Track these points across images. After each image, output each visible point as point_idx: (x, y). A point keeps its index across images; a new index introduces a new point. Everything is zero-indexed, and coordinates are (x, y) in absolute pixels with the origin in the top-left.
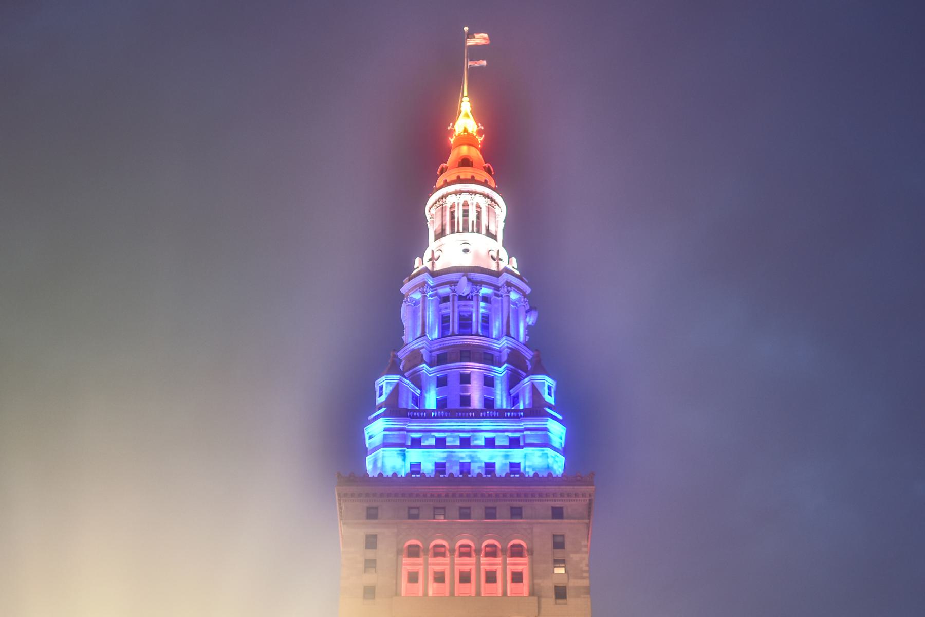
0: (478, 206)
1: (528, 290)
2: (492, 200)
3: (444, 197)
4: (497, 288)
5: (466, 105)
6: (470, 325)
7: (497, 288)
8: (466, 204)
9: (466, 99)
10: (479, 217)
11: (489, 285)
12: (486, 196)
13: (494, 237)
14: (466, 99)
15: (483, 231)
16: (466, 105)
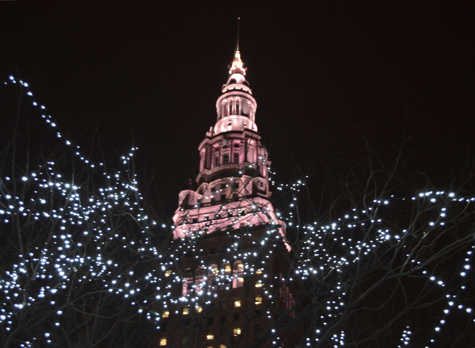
0: (238, 101)
1: (259, 138)
2: (245, 97)
3: (222, 100)
4: (241, 139)
5: (238, 55)
6: (228, 160)
7: (241, 139)
8: (231, 102)
9: (238, 52)
10: (238, 107)
11: (237, 138)
12: (241, 96)
13: (247, 116)
14: (238, 52)
15: (240, 113)
16: (238, 55)
